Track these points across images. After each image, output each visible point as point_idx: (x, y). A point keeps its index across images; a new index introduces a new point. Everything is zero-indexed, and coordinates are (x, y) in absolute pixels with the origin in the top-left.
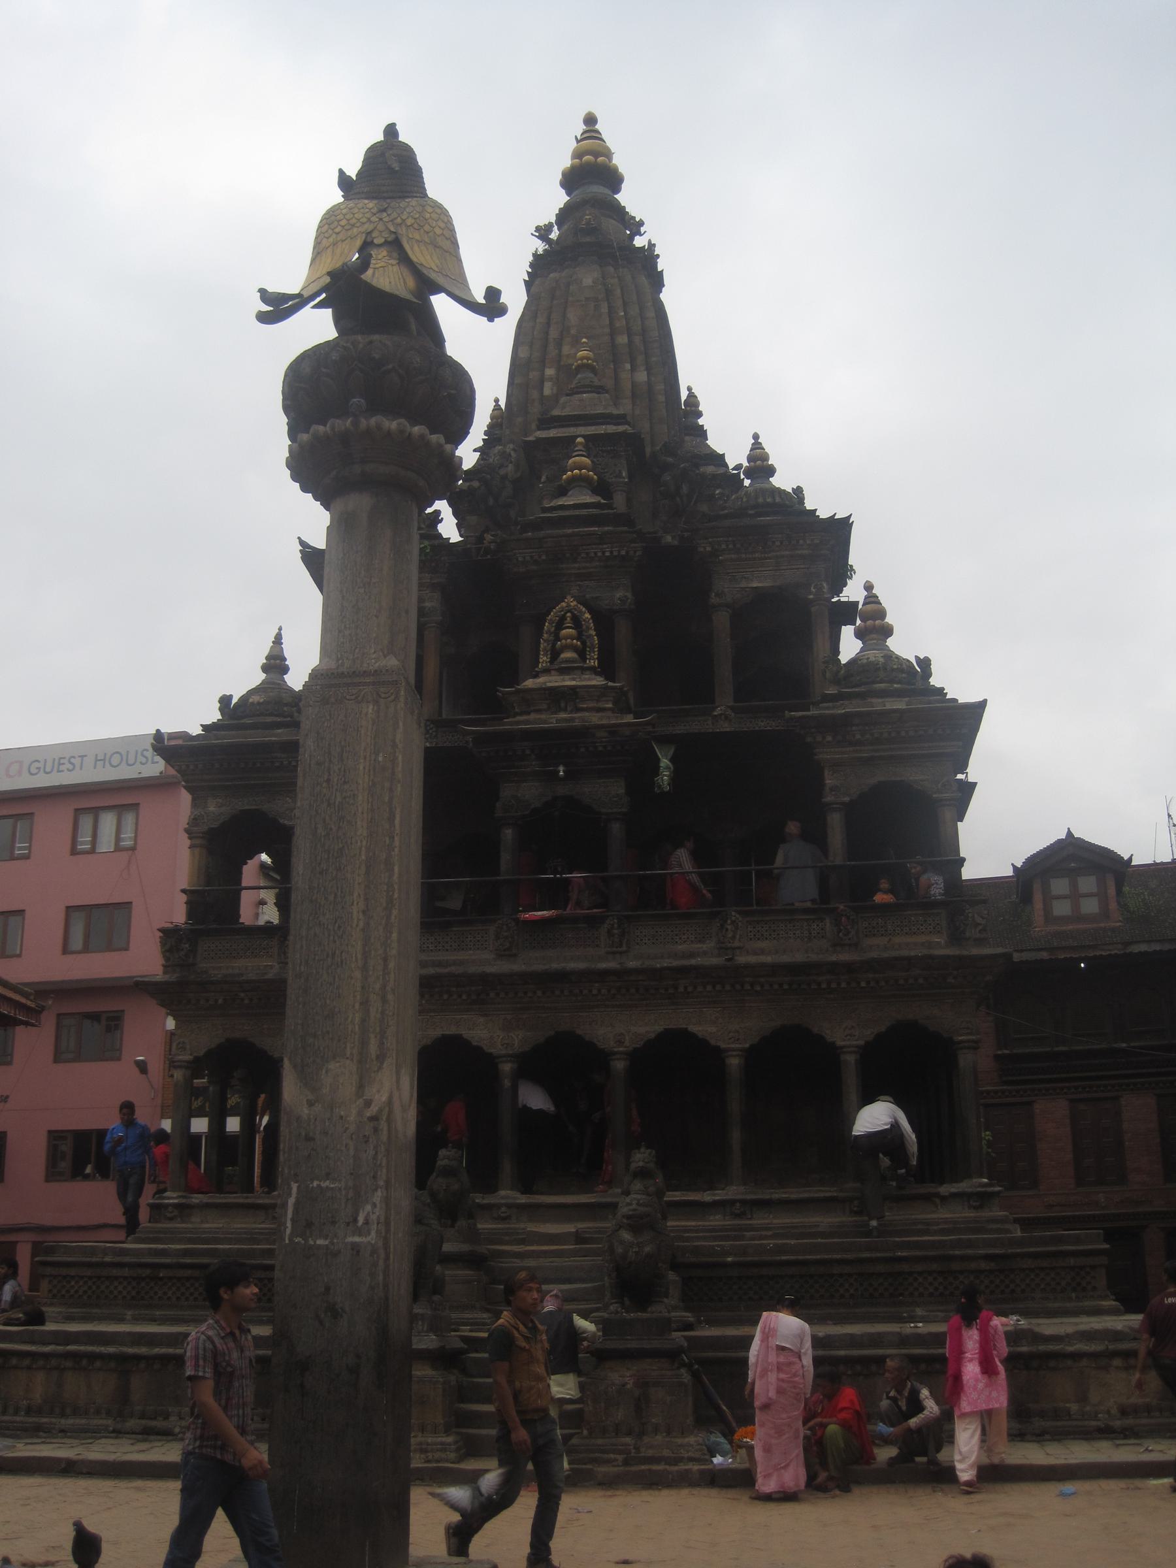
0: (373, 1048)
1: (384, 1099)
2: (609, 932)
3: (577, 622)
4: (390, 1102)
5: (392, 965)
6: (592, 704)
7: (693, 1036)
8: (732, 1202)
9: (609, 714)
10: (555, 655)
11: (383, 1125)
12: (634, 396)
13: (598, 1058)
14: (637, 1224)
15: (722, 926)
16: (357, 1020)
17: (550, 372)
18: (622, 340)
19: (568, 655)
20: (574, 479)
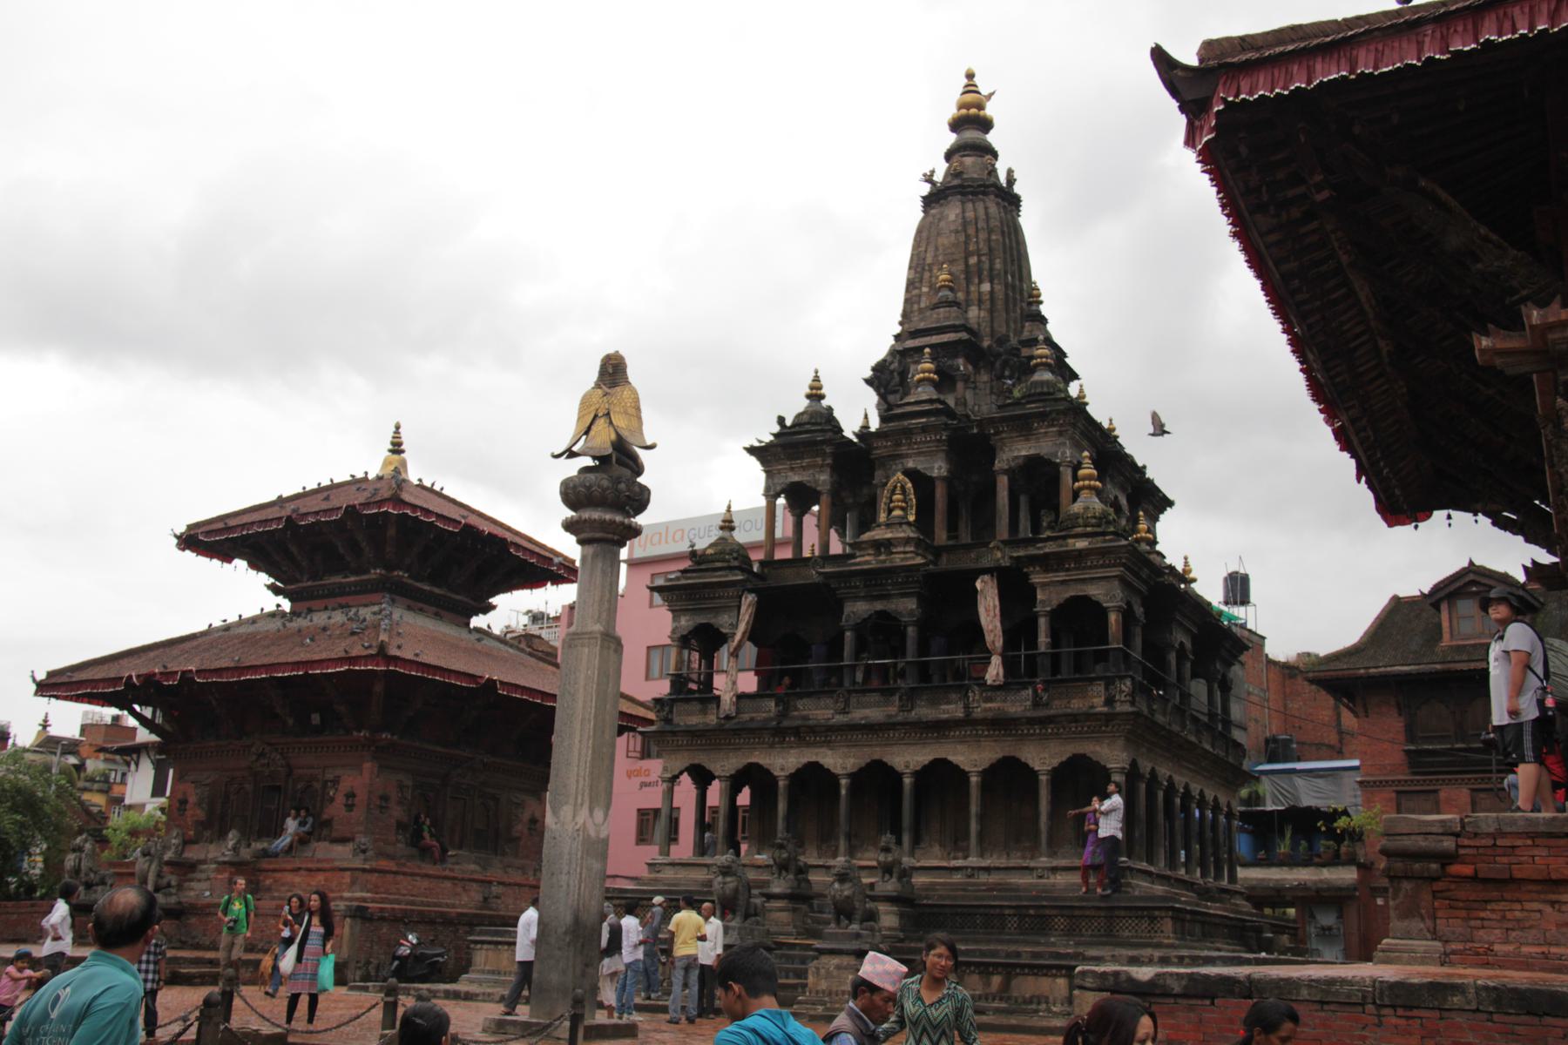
3: (903, 488)
7: (950, 762)
10: (890, 511)
13: (897, 777)
14: (842, 878)
17: (925, 289)
18: (973, 260)
19: (897, 513)
20: (920, 380)
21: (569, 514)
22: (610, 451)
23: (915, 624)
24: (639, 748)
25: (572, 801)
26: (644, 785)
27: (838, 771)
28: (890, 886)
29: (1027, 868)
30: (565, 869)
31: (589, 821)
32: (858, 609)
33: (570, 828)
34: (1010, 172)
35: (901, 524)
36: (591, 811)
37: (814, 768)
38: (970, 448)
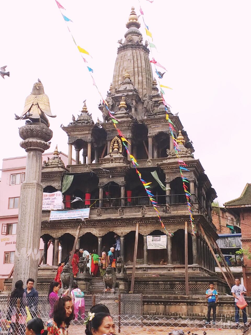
0: (29, 246)
1: (30, 253)
2: (120, 210)
3: (118, 142)
4: (31, 254)
5: (32, 232)
6: (119, 161)
8: (143, 268)
9: (122, 163)
10: (113, 149)
11: (30, 258)
12: (138, 83)
15: (142, 209)
16: (27, 241)
17: (120, 78)
18: (136, 69)
19: (116, 149)
21: (21, 140)
22: (39, 117)
23: (124, 186)
24: (5, 231)
25: (26, 246)
26: (6, 243)
27: (98, 235)
28: (120, 275)
29: (164, 268)
30: (23, 272)
31: (32, 253)
32: (104, 181)
33: (25, 257)
34: (146, 42)
35: (118, 153)
36: (33, 249)
37: (89, 234)
38: (139, 130)
